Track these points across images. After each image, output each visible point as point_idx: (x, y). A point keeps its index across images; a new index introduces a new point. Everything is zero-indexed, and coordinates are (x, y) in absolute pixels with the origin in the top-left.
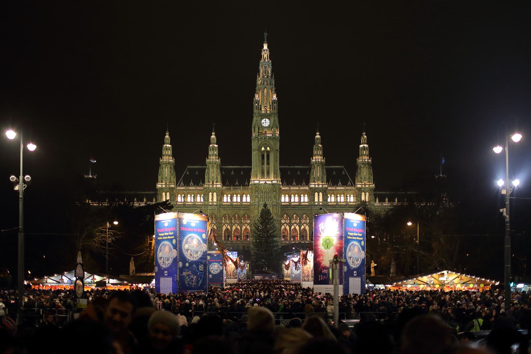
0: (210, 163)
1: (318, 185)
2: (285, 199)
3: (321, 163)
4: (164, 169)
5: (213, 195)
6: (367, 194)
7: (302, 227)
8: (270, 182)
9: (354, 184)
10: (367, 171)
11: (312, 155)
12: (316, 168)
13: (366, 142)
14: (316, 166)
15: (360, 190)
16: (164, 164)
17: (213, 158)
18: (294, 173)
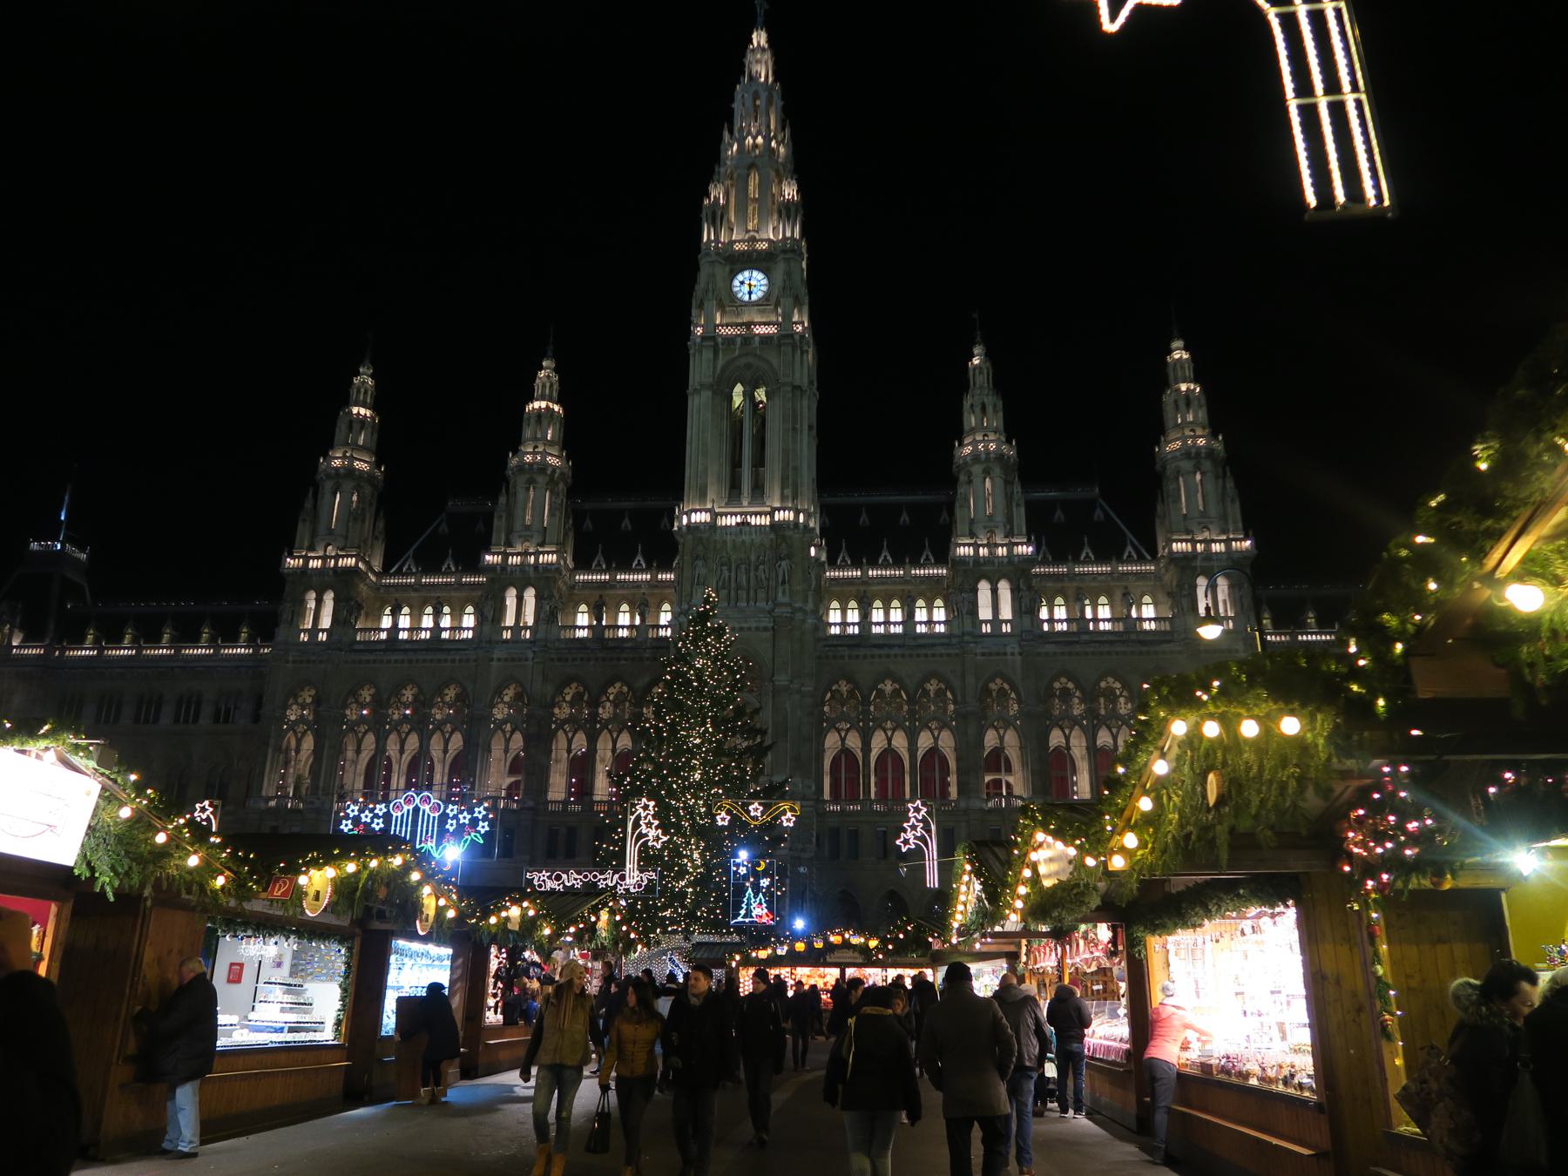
0: (522, 468)
1: (992, 546)
2: (841, 618)
3: (1000, 457)
4: (328, 496)
5: (520, 599)
6: (1223, 584)
7: (925, 741)
8: (765, 521)
9: (1149, 549)
10: (1210, 487)
11: (958, 433)
12: (977, 481)
13: (1189, 373)
14: (977, 469)
15: (1188, 566)
16: (328, 476)
17: (541, 451)
18: (884, 498)
